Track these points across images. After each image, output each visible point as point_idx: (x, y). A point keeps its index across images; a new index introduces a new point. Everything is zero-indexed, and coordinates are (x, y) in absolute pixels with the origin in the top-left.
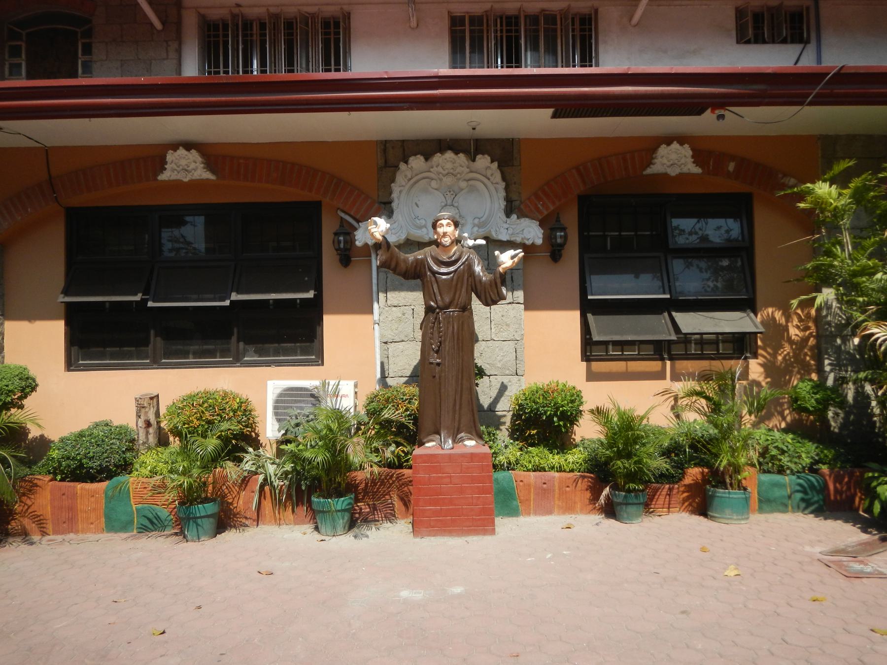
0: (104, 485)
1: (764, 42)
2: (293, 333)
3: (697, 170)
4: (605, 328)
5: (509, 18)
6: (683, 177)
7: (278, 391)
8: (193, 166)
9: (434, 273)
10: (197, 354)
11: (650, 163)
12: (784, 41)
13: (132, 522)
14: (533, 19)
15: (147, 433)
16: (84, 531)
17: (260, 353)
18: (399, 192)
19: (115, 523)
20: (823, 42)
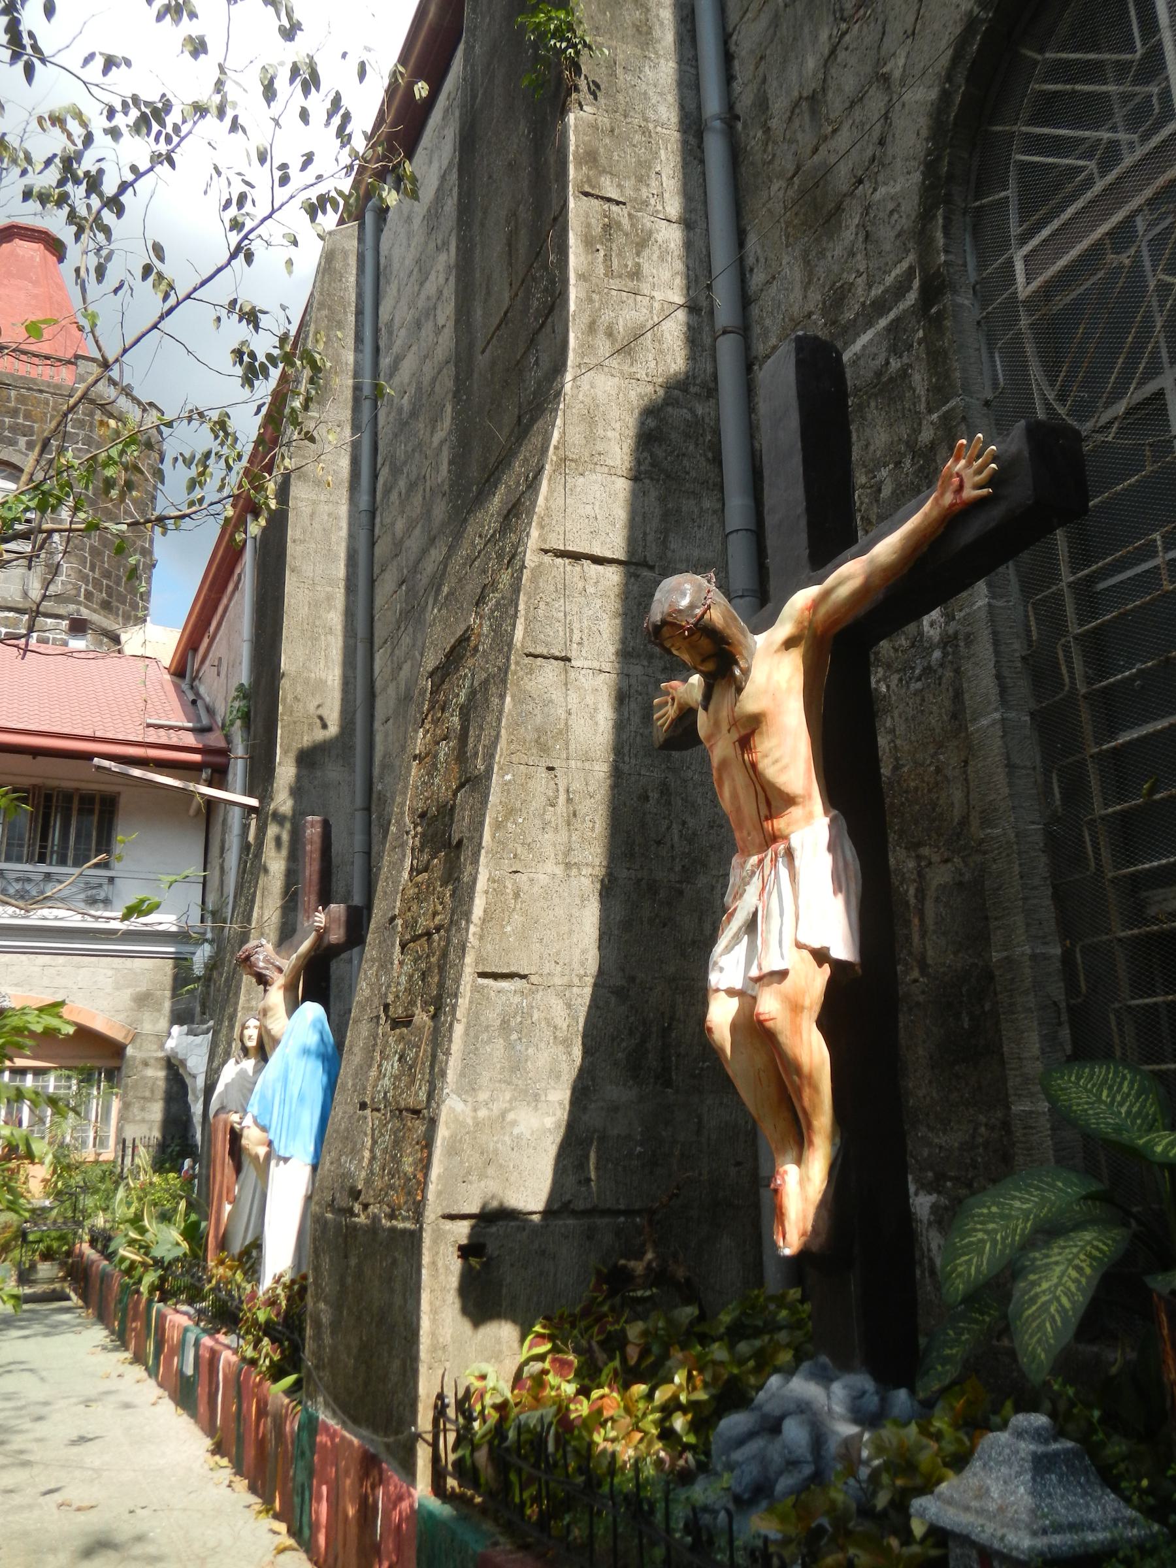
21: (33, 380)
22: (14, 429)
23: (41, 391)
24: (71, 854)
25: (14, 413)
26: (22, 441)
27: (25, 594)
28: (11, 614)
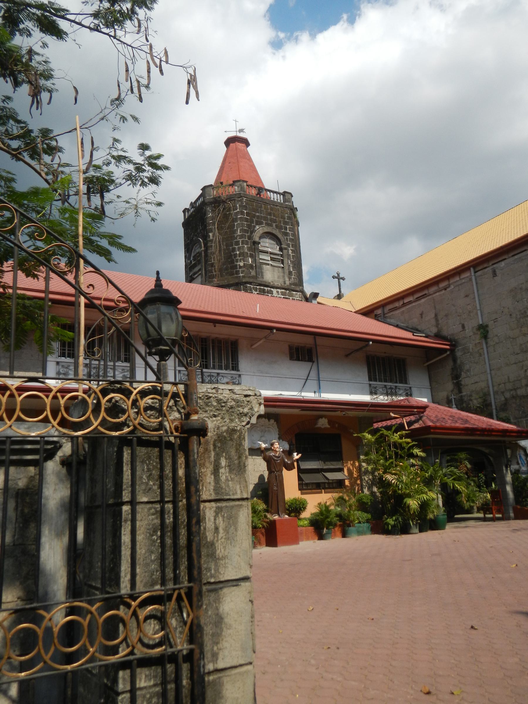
3: (329, 427)
4: (308, 478)
6: (326, 429)
9: (274, 460)
11: (316, 424)
12: (305, 361)
14: (213, 341)
21: (273, 201)
22: (271, 220)
23: (277, 206)
25: (270, 214)
26: (274, 224)
27: (285, 283)
28: (283, 291)
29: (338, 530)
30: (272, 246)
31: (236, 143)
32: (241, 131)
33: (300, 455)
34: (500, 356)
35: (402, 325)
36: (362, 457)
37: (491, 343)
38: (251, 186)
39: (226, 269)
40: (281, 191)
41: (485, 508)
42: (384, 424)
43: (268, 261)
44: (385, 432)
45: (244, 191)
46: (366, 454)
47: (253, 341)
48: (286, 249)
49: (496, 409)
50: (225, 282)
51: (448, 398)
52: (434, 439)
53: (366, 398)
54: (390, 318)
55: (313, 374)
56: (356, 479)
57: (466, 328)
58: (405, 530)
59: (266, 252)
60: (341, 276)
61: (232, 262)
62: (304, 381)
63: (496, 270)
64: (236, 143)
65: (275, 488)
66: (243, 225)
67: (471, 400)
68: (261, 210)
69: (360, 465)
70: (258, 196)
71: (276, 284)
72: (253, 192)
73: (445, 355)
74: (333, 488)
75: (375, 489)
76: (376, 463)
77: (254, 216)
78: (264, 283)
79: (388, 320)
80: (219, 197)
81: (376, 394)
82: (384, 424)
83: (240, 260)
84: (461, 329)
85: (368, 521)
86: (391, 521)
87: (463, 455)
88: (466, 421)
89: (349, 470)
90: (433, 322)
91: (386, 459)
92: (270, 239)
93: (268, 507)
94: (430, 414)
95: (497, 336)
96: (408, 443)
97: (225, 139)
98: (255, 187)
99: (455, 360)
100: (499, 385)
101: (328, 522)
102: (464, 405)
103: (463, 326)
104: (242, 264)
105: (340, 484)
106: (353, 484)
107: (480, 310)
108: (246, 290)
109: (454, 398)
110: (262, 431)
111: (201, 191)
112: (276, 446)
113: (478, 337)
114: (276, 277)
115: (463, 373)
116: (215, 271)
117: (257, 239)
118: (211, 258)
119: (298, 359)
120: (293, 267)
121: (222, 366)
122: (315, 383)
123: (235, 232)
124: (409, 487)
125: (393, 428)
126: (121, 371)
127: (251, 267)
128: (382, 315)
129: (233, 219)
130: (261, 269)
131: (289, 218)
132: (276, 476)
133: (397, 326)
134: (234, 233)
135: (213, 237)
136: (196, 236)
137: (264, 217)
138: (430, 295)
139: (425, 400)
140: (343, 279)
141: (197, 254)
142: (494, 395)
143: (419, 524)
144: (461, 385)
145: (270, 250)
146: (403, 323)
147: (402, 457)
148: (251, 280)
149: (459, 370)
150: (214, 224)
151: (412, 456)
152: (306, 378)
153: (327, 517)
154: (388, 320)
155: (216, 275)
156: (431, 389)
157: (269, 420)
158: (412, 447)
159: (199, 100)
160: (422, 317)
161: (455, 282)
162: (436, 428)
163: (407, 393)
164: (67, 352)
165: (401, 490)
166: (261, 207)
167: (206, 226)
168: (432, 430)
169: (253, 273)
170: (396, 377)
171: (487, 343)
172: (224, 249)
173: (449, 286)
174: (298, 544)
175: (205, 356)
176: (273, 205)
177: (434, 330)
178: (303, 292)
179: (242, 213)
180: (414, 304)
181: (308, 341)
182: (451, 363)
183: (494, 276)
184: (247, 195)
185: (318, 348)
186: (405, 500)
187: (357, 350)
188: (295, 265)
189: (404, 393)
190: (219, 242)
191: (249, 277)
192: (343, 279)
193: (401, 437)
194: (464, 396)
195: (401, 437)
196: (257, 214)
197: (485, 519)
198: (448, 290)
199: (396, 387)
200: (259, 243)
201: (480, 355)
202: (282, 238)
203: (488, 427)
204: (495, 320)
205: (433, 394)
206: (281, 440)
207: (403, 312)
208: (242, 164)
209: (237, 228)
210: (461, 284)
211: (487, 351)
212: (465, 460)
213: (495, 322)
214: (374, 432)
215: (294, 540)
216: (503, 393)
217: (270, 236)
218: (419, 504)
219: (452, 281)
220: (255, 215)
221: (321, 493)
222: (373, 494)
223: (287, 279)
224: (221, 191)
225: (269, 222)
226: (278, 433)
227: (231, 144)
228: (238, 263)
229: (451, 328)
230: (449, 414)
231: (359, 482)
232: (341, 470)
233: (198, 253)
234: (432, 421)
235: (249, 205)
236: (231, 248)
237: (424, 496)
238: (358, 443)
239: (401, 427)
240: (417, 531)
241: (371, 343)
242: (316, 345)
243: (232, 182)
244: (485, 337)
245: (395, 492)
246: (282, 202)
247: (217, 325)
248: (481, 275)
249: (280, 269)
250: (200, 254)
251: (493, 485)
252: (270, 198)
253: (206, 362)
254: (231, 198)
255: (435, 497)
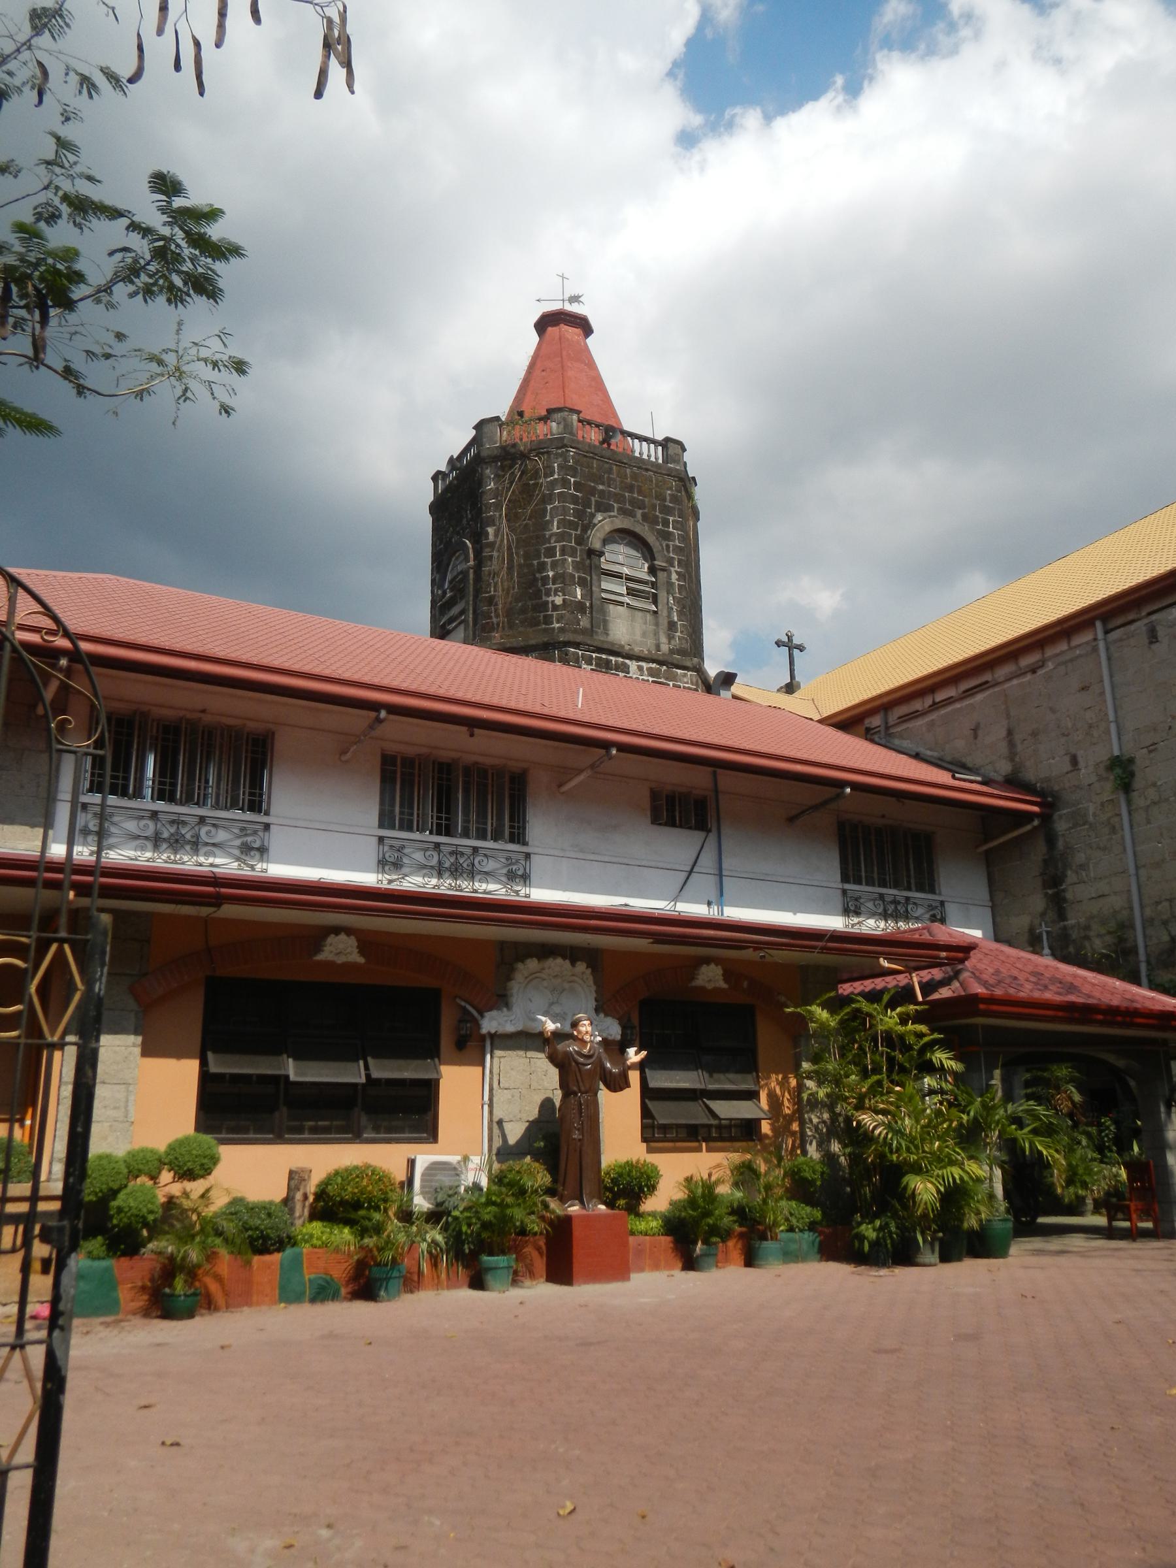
0: (277, 1257)
1: (673, 825)
2: (415, 1112)
3: (722, 985)
4: (665, 1113)
5: (441, 764)
7: (426, 1165)
8: (349, 950)
9: (577, 1063)
10: (314, 1130)
11: (693, 979)
12: (690, 828)
13: (305, 1293)
14: (468, 770)
15: (304, 1207)
16: (259, 1304)
17: (377, 1129)
18: (515, 987)
19: (289, 1295)
20: (723, 832)
21: (640, 459)
22: (633, 502)
23: (647, 470)
24: (913, 881)
25: (630, 488)
26: (639, 513)
27: (658, 647)
28: (654, 665)
29: (734, 1247)
30: (632, 562)
31: (561, 326)
32: (575, 299)
33: (644, 1053)
34: (1161, 834)
35: (929, 753)
36: (806, 1065)
37: (1139, 801)
38: (589, 423)
39: (523, 611)
40: (660, 437)
41: (1112, 1203)
42: (868, 985)
43: (622, 595)
44: (865, 1006)
45: (571, 433)
46: (816, 1059)
47: (562, 774)
48: (664, 570)
49: (1148, 962)
50: (520, 641)
51: (1031, 930)
52: (986, 1028)
53: (835, 923)
54: (901, 737)
55: (708, 860)
56: (789, 1119)
57: (1082, 764)
58: (903, 1254)
59: (618, 576)
60: (796, 641)
61: (537, 594)
62: (684, 875)
63: (1158, 628)
64: (561, 326)
65: (576, 1135)
66: (565, 511)
67: (1087, 938)
68: (609, 479)
69: (801, 1087)
70: (605, 445)
71: (637, 649)
72: (594, 436)
73: (1029, 827)
74: (732, 1139)
75: (835, 1147)
76: (837, 1082)
77: (593, 491)
78: (610, 647)
79: (897, 742)
80: (514, 445)
81: (857, 913)
82: (868, 985)
83: (556, 590)
84: (1067, 766)
85: (812, 1226)
86: (869, 1231)
87: (1062, 1071)
88: (1071, 988)
89: (772, 1096)
90: (1003, 748)
91: (865, 1074)
92: (627, 545)
93: (555, 1181)
94: (981, 966)
95: (1154, 785)
96: (920, 1035)
97: (536, 317)
98: (597, 426)
99: (1051, 840)
100: (1158, 903)
101: (709, 1225)
102: (1071, 949)
103: (1074, 761)
104: (558, 600)
105: (747, 1130)
106: (781, 1130)
107: (1116, 722)
108: (565, 660)
109: (1047, 932)
110: (553, 990)
111: (474, 432)
112: (583, 1029)
113: (1109, 786)
114: (638, 632)
115: (1069, 873)
116: (497, 616)
117: (597, 545)
118: (490, 584)
119: (671, 823)
120: (680, 613)
121: (485, 830)
122: (712, 880)
123: (546, 525)
124: (916, 1147)
125: (886, 998)
126: (236, 831)
127: (581, 607)
128: (882, 729)
129: (544, 496)
130: (604, 612)
131: (674, 499)
132: (581, 1104)
133: (917, 756)
134: (544, 529)
135: (496, 535)
136: (458, 533)
137: (615, 494)
138: (997, 684)
139: (977, 934)
140: (801, 648)
141: (458, 574)
142: (1144, 928)
143: (941, 1241)
144: (1065, 900)
145: (626, 571)
146: (931, 750)
147: (903, 1070)
148: (579, 638)
149: (1060, 865)
150: (498, 506)
151: (929, 1068)
152: (688, 868)
153: (707, 1214)
154: (897, 742)
155: (498, 624)
156: (993, 908)
157: (573, 964)
158: (930, 1046)
159: (353, 92)
160: (976, 737)
161: (1057, 655)
162: (991, 1000)
163: (934, 916)
164: (108, 780)
165: (898, 1150)
166: (610, 471)
167: (480, 512)
168: (982, 1006)
169: (584, 622)
170: (909, 876)
171: (1129, 802)
172: (520, 566)
173: (1042, 664)
174: (628, 1279)
175: (445, 804)
176: (639, 468)
177: (1005, 768)
178: (700, 671)
179: (565, 483)
180: (958, 705)
181: (698, 779)
182: (1040, 849)
183: (1151, 643)
184: (578, 442)
185: (720, 797)
186: (905, 1179)
187: (815, 808)
188: (684, 607)
189: (927, 916)
190: (509, 548)
191: (575, 631)
192: (801, 648)
193: (904, 1020)
194: (1073, 927)
195: (904, 1020)
196: (601, 487)
197: (1109, 1233)
198: (1041, 672)
199: (907, 899)
200: (601, 554)
201: (1113, 830)
202: (658, 544)
203: (1125, 1004)
204: (1152, 748)
205: (998, 919)
206: (602, 1015)
207: (932, 724)
208: (570, 373)
209: (552, 518)
210: (1071, 660)
211: (1131, 821)
212: (1068, 1083)
213: (1150, 752)
214: (834, 1005)
215: (618, 1270)
216: (1165, 923)
217: (629, 538)
218: (938, 1191)
219: (1050, 652)
220: (594, 488)
221: (699, 1150)
222: (830, 1159)
223: (663, 639)
224: (517, 432)
225: (628, 506)
226: (594, 995)
227: (550, 329)
228: (550, 599)
229: (1046, 764)
230: (1030, 968)
231: (795, 1127)
232: (752, 1095)
233: (462, 572)
234: (985, 984)
235: (582, 465)
236: (535, 562)
237: (956, 1172)
238: (797, 1028)
239: (904, 995)
240: (935, 1258)
241: (848, 790)
242: (716, 791)
243: (544, 413)
244: (1126, 786)
245: (882, 1156)
246: (660, 461)
247: (476, 731)
248: (1121, 640)
249: (649, 617)
250: (465, 573)
251: (1136, 1149)
252: (633, 451)
253: (447, 819)
254: (542, 448)
255: (987, 1174)
